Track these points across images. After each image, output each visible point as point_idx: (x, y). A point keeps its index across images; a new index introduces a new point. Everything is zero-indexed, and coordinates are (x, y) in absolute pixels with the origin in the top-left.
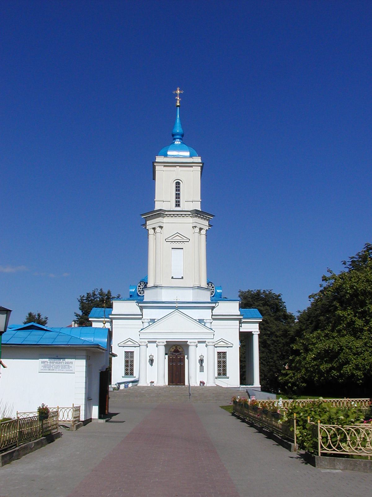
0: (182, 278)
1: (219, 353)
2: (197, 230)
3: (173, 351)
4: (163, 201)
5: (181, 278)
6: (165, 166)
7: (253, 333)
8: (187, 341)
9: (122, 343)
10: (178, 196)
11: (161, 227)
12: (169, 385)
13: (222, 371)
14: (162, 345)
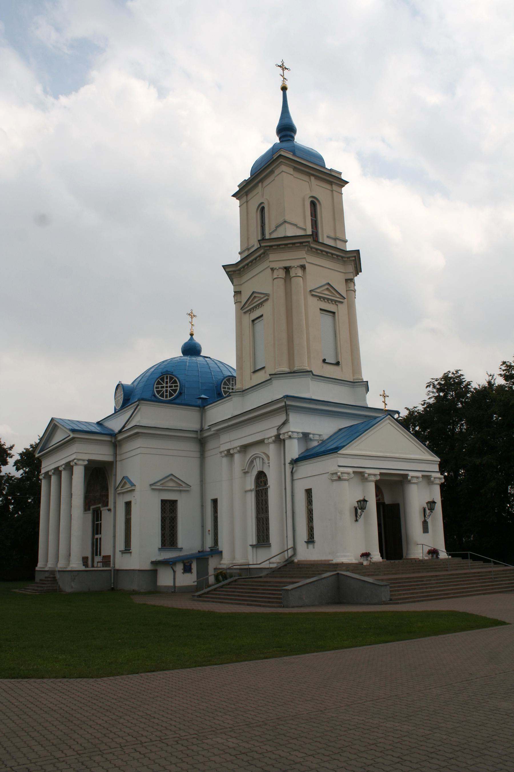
6: (295, 169)
8: (407, 475)
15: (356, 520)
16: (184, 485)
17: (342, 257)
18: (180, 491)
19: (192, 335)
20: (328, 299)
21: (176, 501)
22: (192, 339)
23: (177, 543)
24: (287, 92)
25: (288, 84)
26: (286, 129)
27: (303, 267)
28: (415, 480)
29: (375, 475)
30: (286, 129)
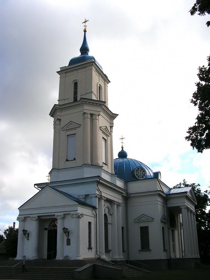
0: (75, 159)
1: (141, 228)
4: (65, 100)
5: (73, 159)
7: (180, 207)
10: (76, 93)
11: (60, 120)
12: (47, 259)
13: (145, 245)
15: (28, 240)
19: (122, 148)
20: (73, 128)
22: (122, 150)
24: (86, 33)
26: (84, 49)
29: (35, 217)
30: (84, 49)
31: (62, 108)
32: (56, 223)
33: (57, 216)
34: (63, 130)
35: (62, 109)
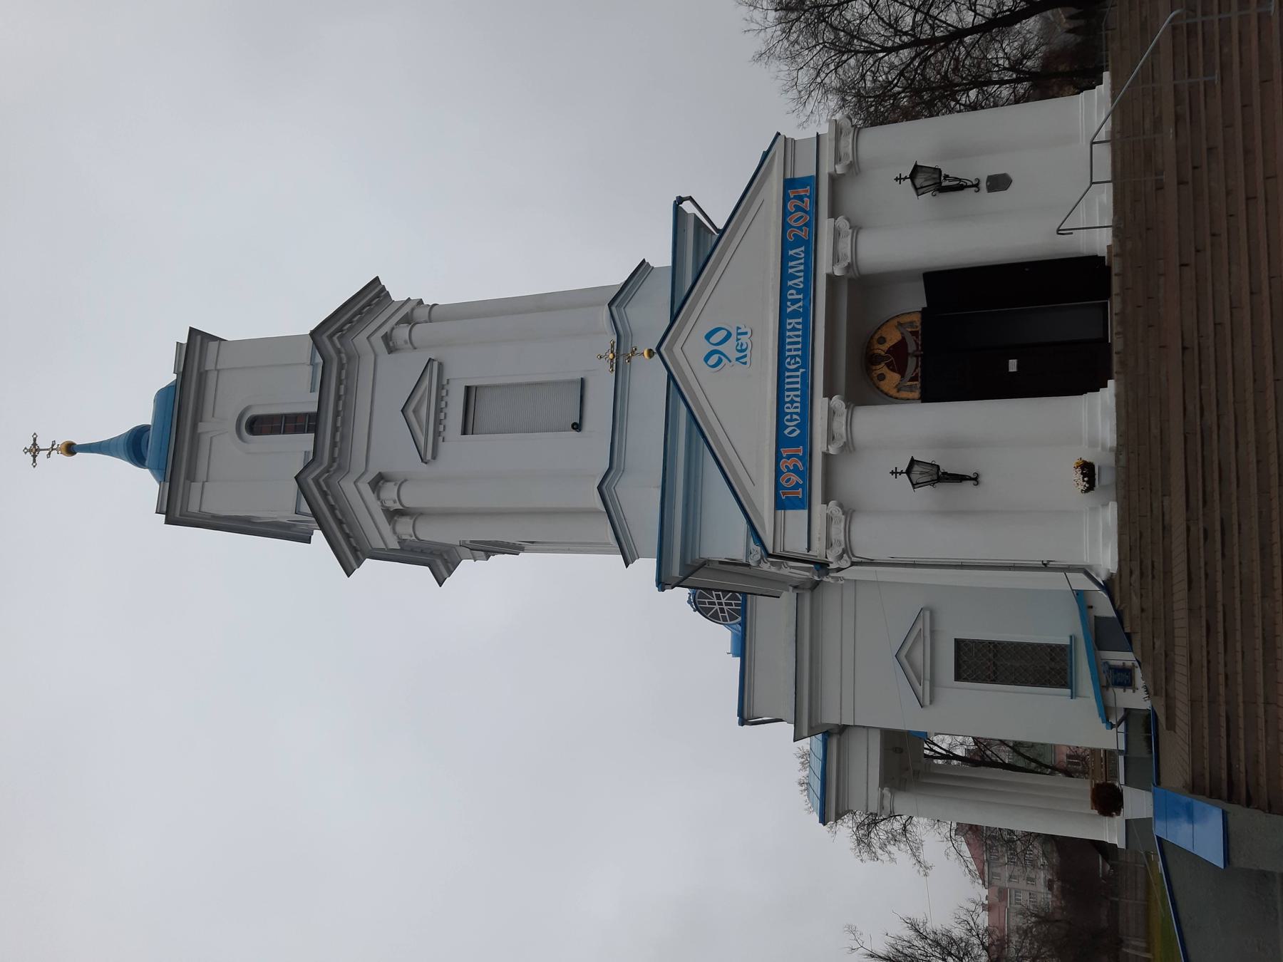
2: (402, 333)
3: (897, 377)
6: (191, 477)
8: (831, 279)
9: (920, 689)
14: (849, 423)
15: (975, 479)
16: (919, 626)
17: (341, 367)
18: (933, 632)
21: (959, 643)
23: (1059, 646)
25: (60, 441)
27: (378, 482)
28: (845, 246)
29: (832, 413)
31: (333, 460)
32: (886, 347)
33: (836, 259)
34: (434, 457)
35: (335, 465)
